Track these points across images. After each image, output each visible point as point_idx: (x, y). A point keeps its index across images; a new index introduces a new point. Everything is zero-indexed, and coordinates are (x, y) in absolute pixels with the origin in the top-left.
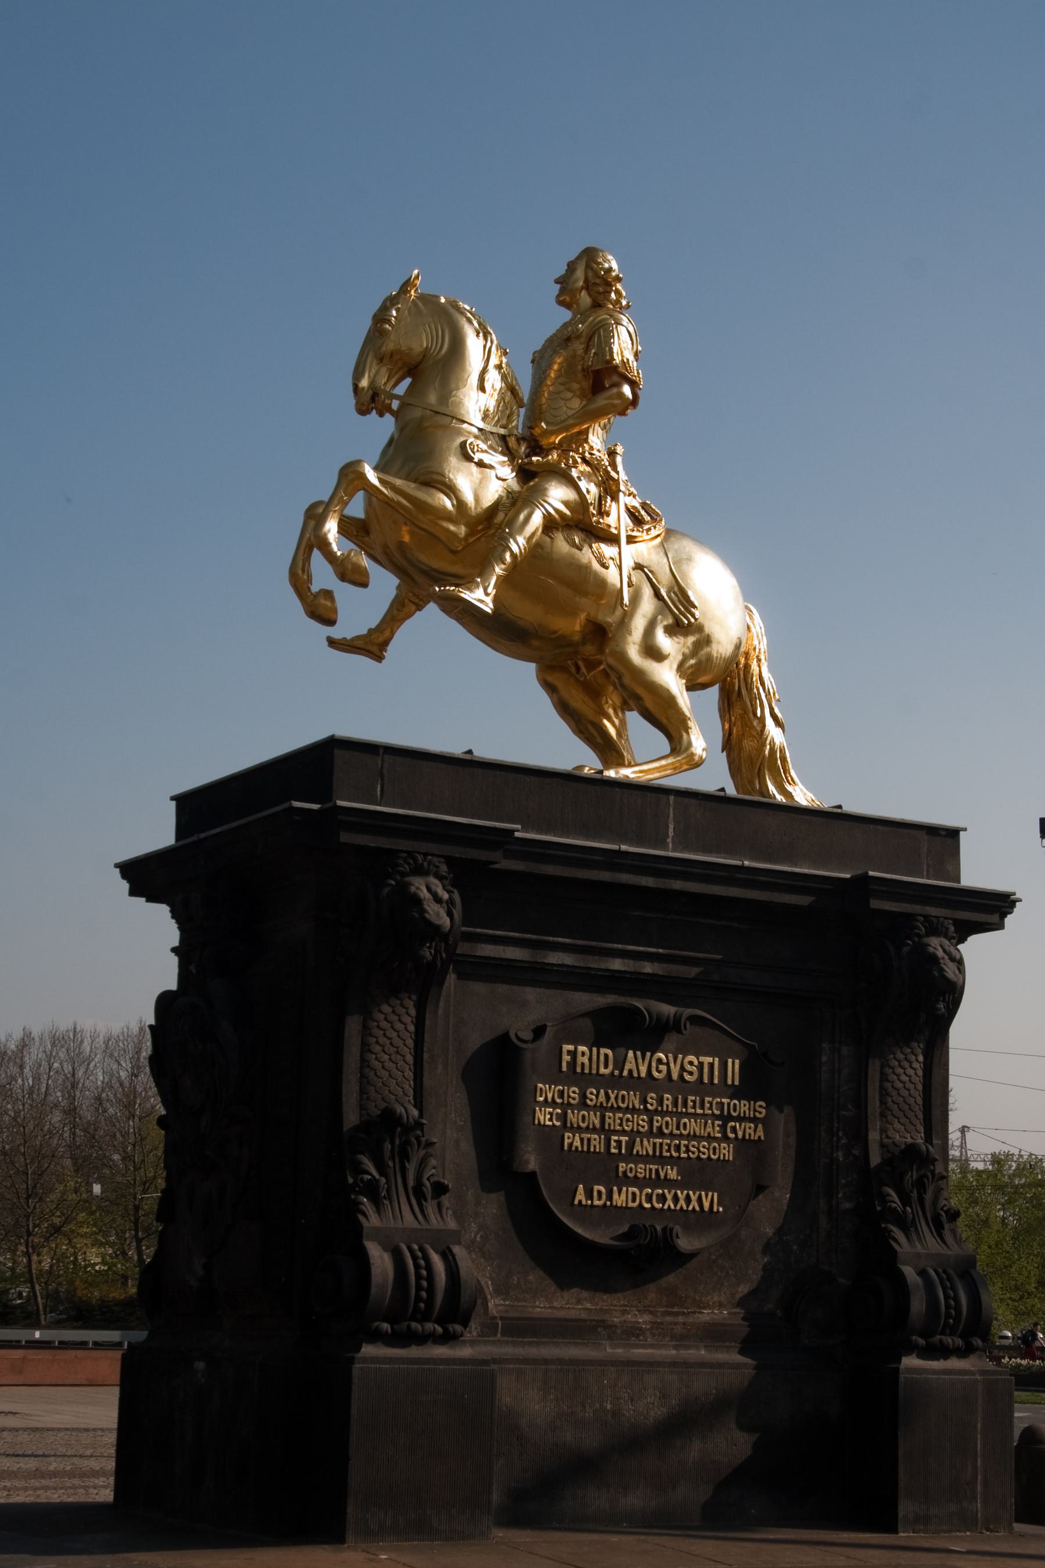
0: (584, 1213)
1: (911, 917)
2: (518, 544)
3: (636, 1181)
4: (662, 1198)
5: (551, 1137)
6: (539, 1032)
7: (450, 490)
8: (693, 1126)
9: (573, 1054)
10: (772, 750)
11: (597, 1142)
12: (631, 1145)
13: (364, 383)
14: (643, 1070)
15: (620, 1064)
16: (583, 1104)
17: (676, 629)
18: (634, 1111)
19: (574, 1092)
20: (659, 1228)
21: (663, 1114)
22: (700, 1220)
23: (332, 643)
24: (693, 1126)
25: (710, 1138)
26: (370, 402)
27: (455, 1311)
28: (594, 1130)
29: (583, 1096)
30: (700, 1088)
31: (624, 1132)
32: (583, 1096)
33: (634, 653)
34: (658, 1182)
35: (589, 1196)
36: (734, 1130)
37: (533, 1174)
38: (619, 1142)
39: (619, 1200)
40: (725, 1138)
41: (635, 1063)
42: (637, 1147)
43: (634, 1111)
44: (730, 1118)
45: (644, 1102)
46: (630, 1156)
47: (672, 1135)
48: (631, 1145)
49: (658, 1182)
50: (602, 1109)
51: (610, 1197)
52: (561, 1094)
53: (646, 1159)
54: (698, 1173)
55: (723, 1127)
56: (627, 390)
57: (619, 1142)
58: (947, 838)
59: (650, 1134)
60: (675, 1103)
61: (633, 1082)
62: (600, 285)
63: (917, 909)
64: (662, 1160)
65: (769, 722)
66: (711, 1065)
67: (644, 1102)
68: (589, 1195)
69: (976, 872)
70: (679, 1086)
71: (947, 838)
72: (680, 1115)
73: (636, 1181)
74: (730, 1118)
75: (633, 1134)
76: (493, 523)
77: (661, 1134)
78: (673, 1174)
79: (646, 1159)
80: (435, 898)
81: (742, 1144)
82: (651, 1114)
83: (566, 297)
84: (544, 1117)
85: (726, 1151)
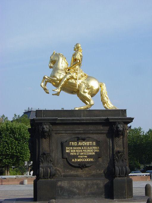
0: (74, 162)
1: (116, 122)
2: (63, 83)
3: (81, 158)
4: (85, 160)
5: (68, 154)
6: (66, 142)
7: (56, 77)
8: (89, 151)
9: (71, 143)
10: (106, 101)
11: (75, 154)
12: (80, 154)
13: (50, 65)
14: (81, 144)
15: (78, 144)
16: (73, 149)
17: (88, 89)
18: (80, 149)
19: (71, 148)
20: (84, 164)
21: (84, 150)
22: (91, 162)
23: (53, 95)
24: (89, 151)
25: (91, 152)
26: (51, 67)
27: (52, 176)
28: (75, 152)
29: (73, 148)
30: (89, 146)
31: (79, 152)
32: (73, 148)
33: (82, 93)
34: (84, 158)
35: (74, 160)
36: (95, 151)
37: (67, 158)
38: (78, 154)
39: (78, 160)
40: (93, 152)
41: (80, 144)
42: (81, 154)
43: (80, 149)
44: (94, 149)
45: (81, 148)
46: (80, 155)
47: (86, 152)
48: (80, 154)
49: (84, 158)
50: (76, 150)
51: (77, 160)
52: (70, 148)
53: (82, 155)
54: (89, 156)
55: (93, 151)
56: (78, 61)
57: (78, 154)
58: (124, 111)
59: (83, 152)
60: (86, 148)
61: (80, 146)
62: (78, 48)
63: (117, 121)
64: (84, 155)
65: (105, 97)
66: (91, 143)
67: (81, 148)
68: (74, 160)
69: (128, 115)
70: (87, 146)
71: (124, 111)
72: (87, 150)
73: (81, 158)
74: (94, 149)
75: (80, 152)
76: (61, 80)
77: (84, 152)
78: (86, 157)
79: (82, 155)
80: (46, 127)
81: (96, 153)
82: (83, 150)
83: (75, 50)
84: (67, 151)
85: (94, 153)
